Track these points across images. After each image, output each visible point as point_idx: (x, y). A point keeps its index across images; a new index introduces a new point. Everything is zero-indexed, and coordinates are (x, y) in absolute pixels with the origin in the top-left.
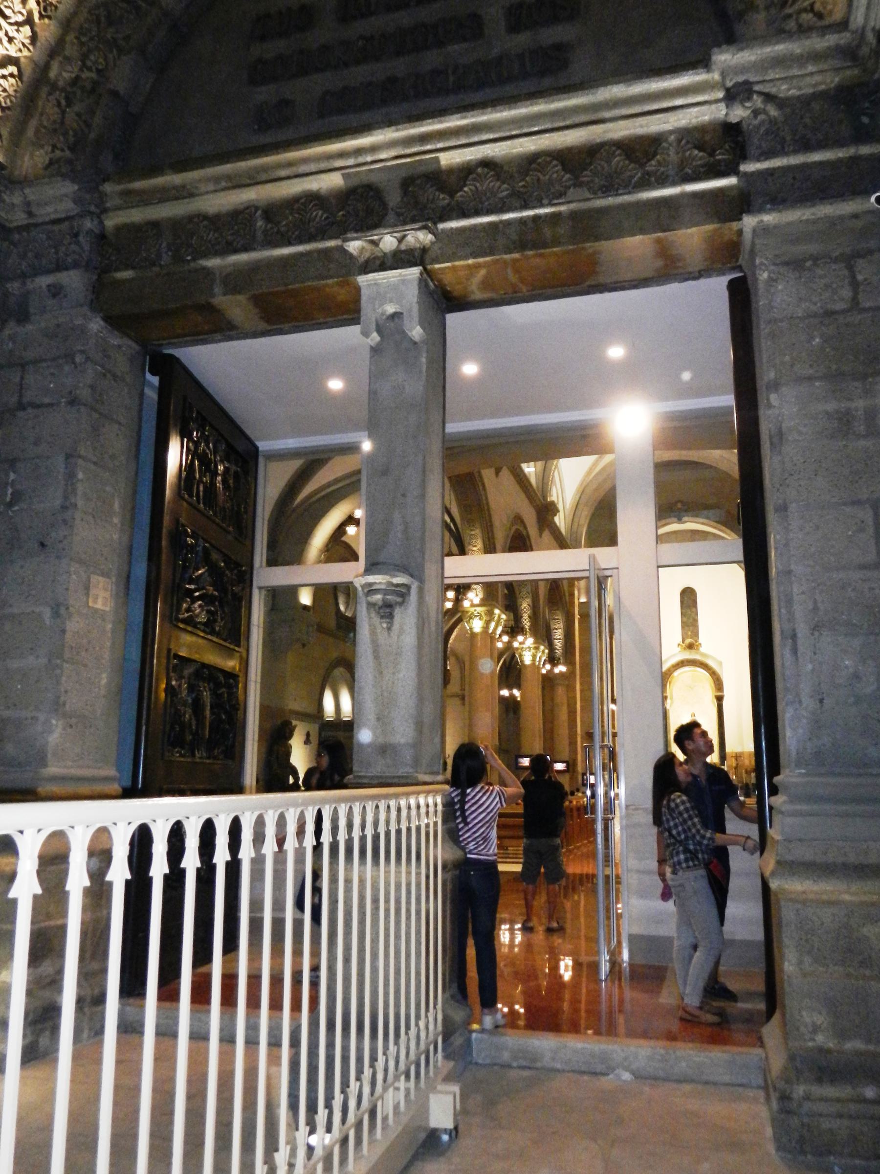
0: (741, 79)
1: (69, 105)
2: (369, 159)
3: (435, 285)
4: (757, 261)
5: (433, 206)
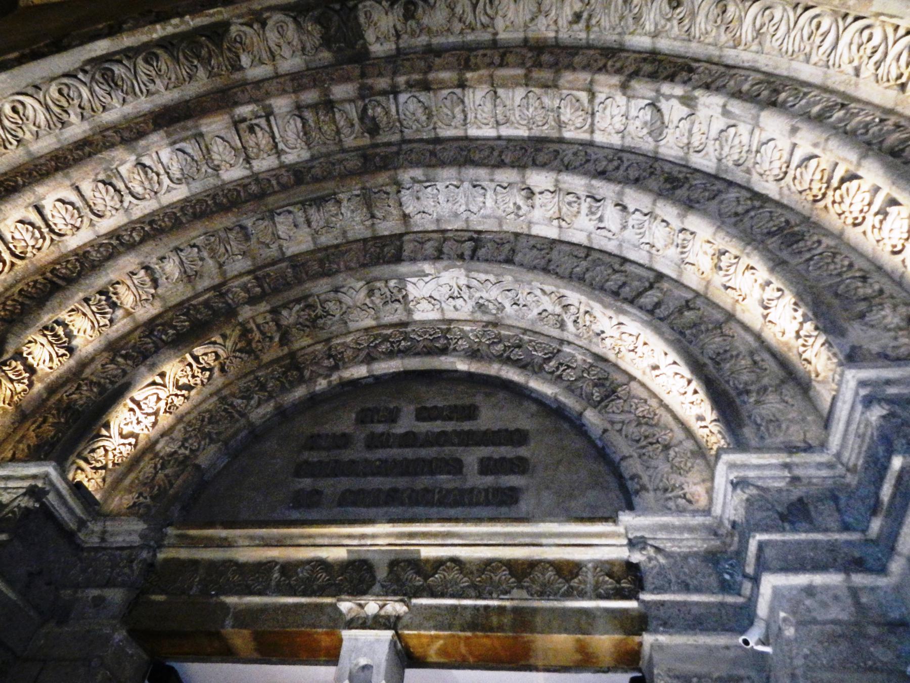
0: (639, 534)
1: (162, 469)
2: (369, 542)
5: (410, 584)
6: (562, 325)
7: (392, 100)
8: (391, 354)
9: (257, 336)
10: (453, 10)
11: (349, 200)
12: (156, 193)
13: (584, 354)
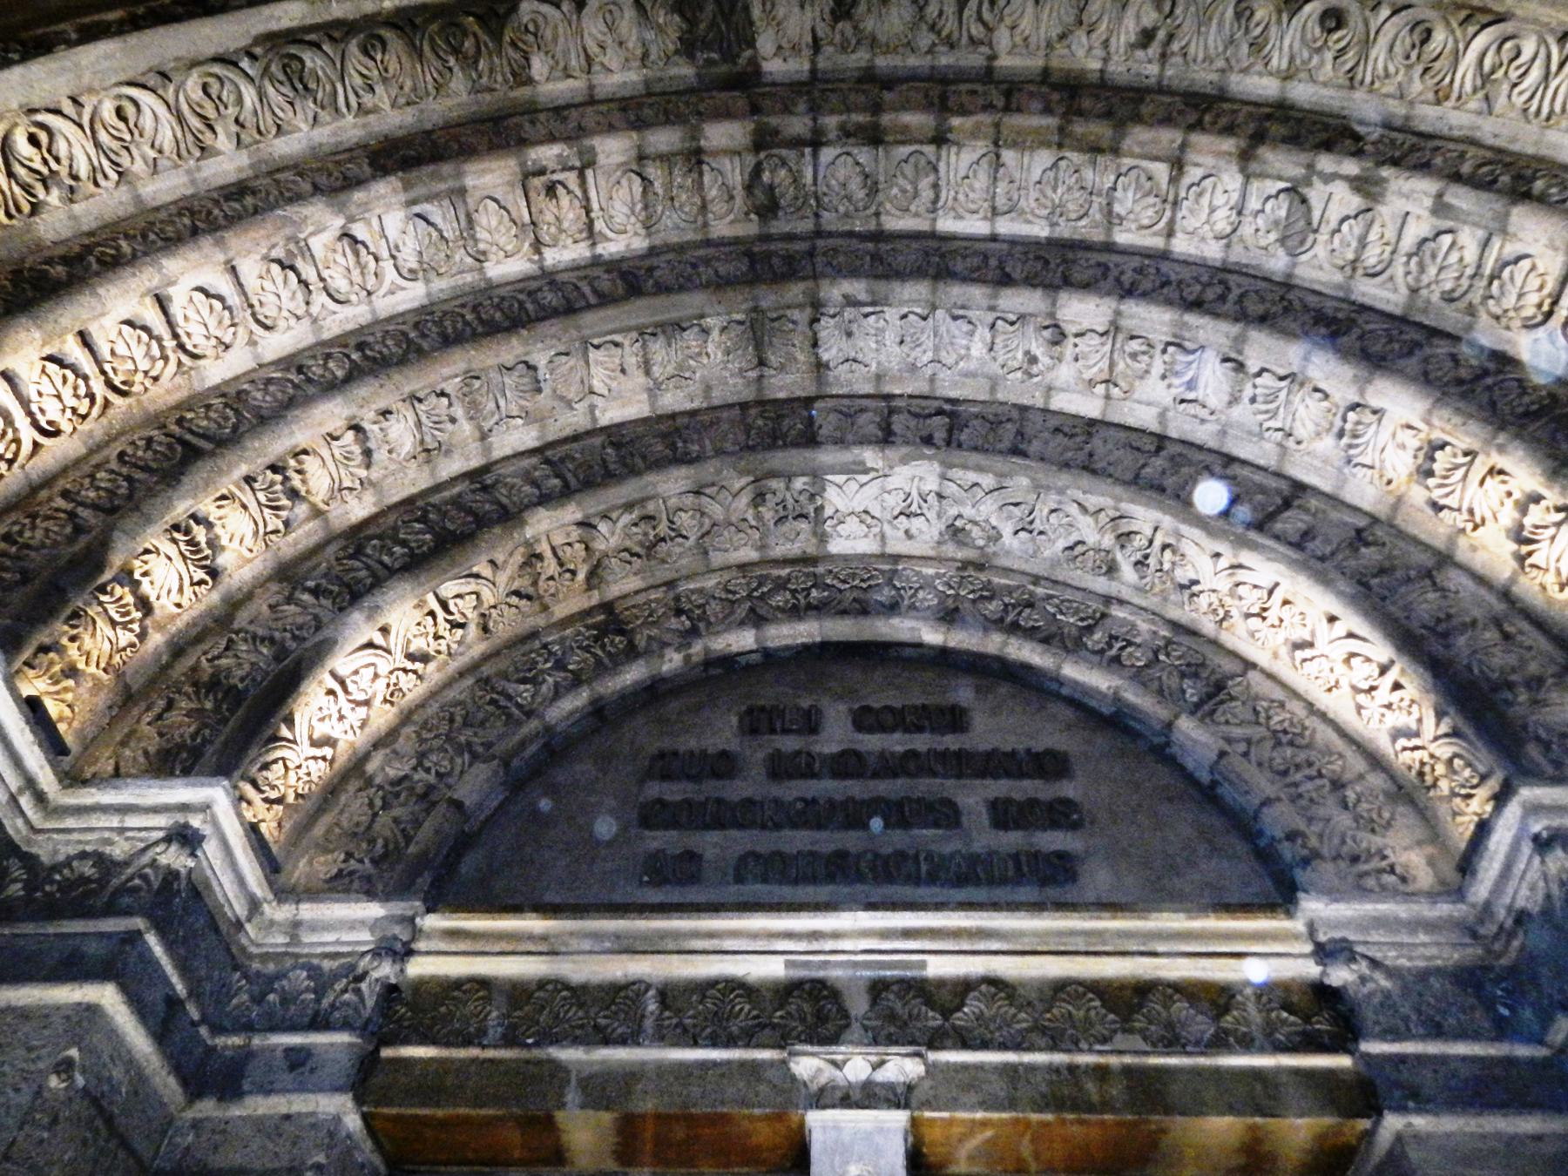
0: (1337, 935)
2: (829, 945)
5: (919, 1025)
6: (1112, 569)
7: (808, 158)
8: (795, 612)
9: (550, 566)
10: (921, 9)
11: (723, 329)
12: (369, 294)
13: (1153, 622)
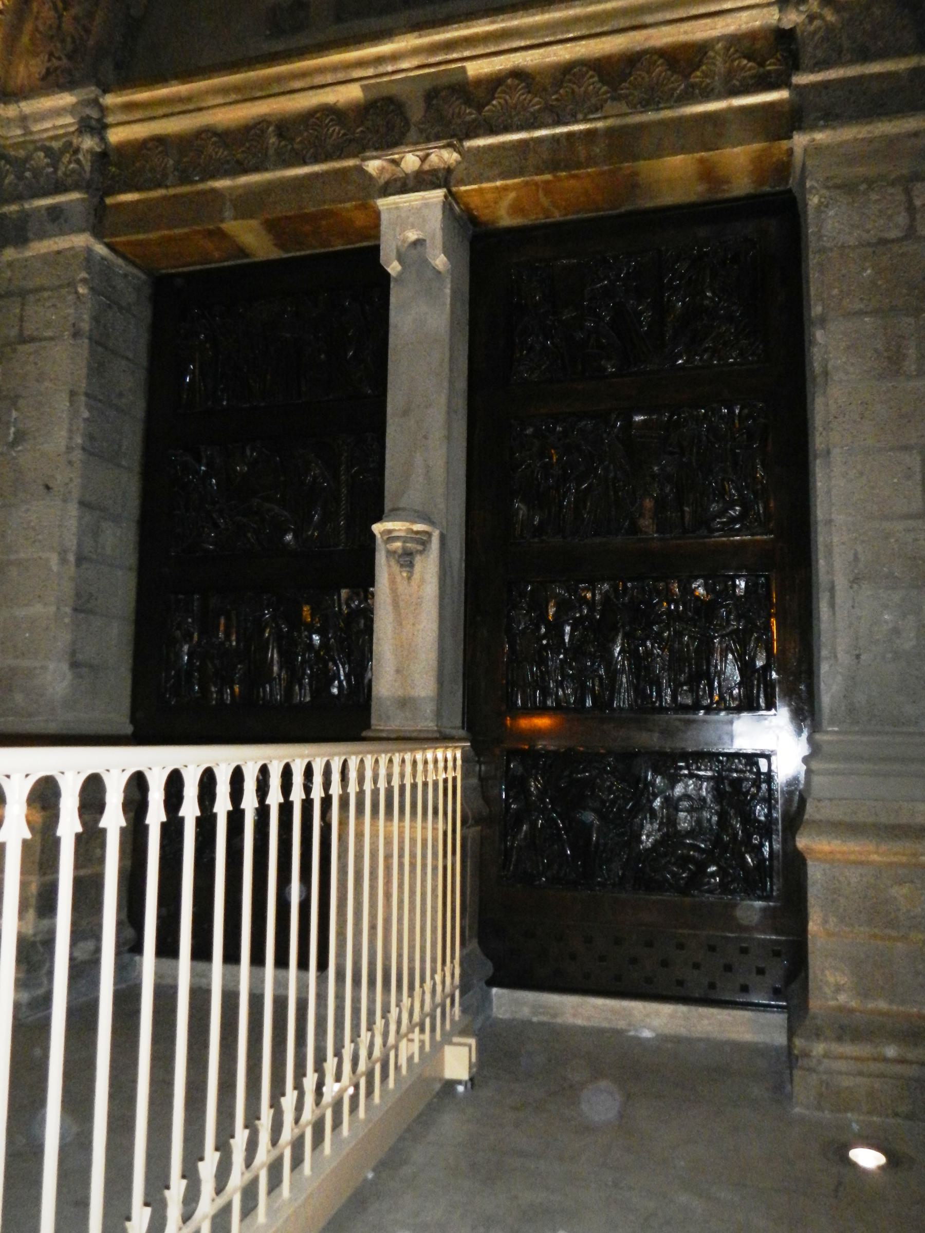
2: (390, 68)
3: (461, 209)
4: (808, 185)
